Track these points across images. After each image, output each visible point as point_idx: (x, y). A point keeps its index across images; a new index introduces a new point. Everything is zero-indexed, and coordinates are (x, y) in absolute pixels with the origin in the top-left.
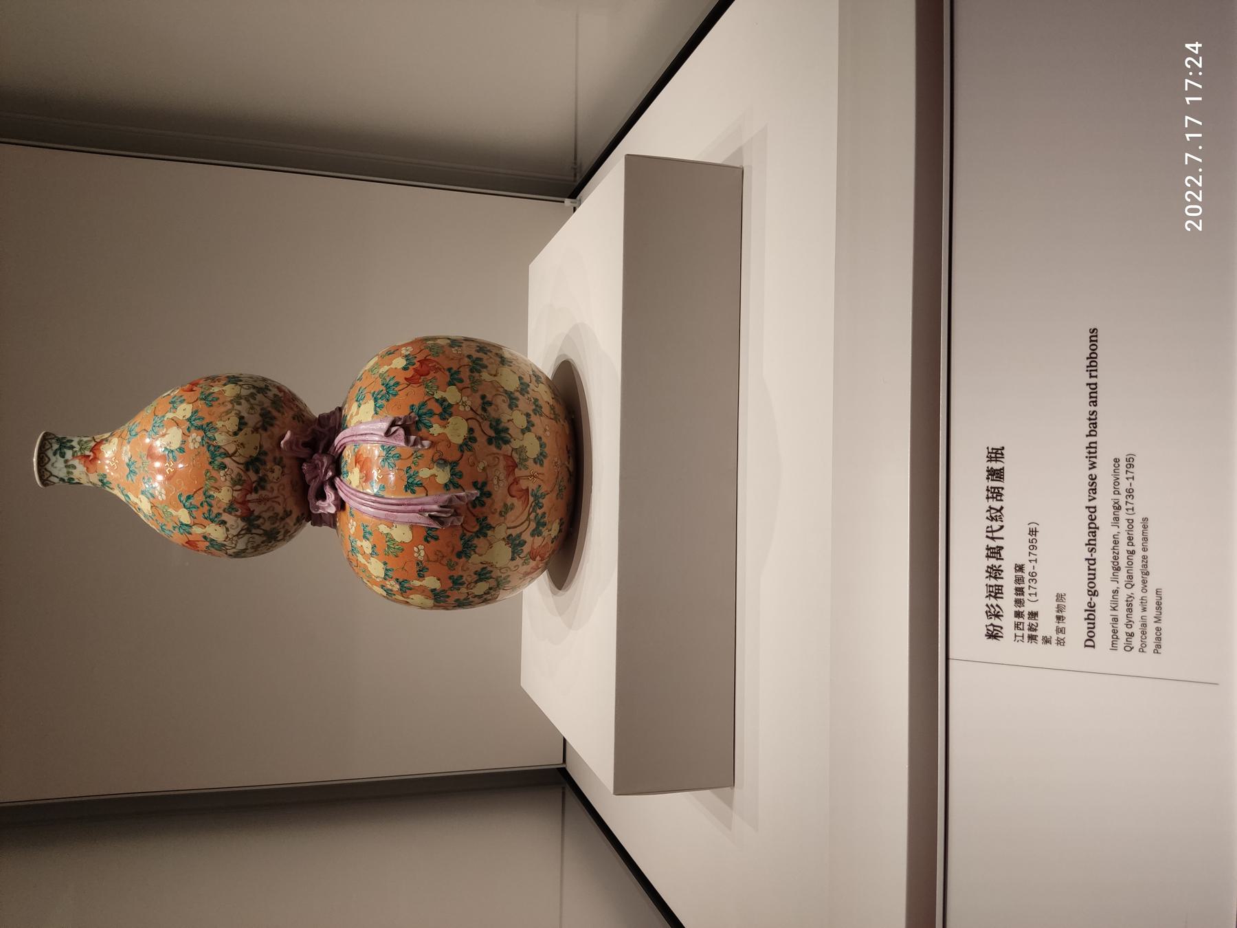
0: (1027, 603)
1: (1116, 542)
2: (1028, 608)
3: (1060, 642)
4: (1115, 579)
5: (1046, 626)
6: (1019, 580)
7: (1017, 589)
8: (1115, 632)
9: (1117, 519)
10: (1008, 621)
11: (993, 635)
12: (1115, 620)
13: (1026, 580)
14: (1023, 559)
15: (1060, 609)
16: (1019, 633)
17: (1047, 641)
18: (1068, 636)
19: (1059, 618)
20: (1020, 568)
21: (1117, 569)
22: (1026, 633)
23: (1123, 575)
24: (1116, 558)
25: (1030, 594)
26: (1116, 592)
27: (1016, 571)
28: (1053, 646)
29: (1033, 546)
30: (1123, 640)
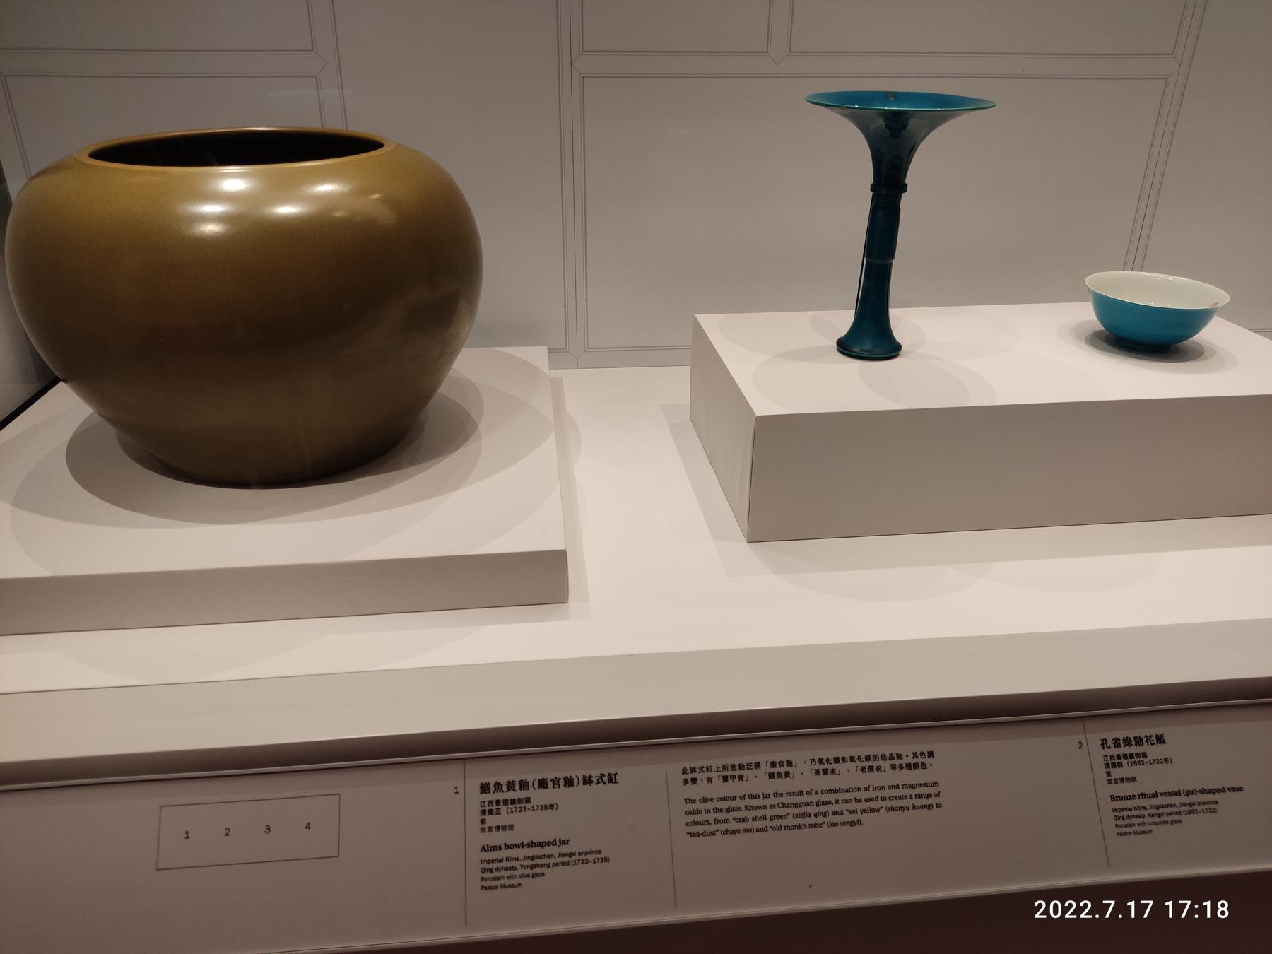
0: (505, 807)
1: (549, 856)
2: (503, 808)
3: (483, 830)
4: (526, 858)
5: (491, 821)
6: (520, 801)
7: (514, 800)
8: (493, 861)
9: (563, 855)
10: (493, 796)
11: (484, 788)
12: (500, 861)
13: (520, 805)
14: (534, 802)
15: (504, 828)
16: (486, 804)
17: (483, 821)
18: (487, 834)
19: (498, 828)
20: (528, 800)
21: (532, 858)
22: (487, 808)
23: (529, 862)
24: (539, 857)
25: (512, 809)
26: (518, 859)
27: (526, 798)
28: (479, 826)
29: (544, 807)
30: (487, 869)
